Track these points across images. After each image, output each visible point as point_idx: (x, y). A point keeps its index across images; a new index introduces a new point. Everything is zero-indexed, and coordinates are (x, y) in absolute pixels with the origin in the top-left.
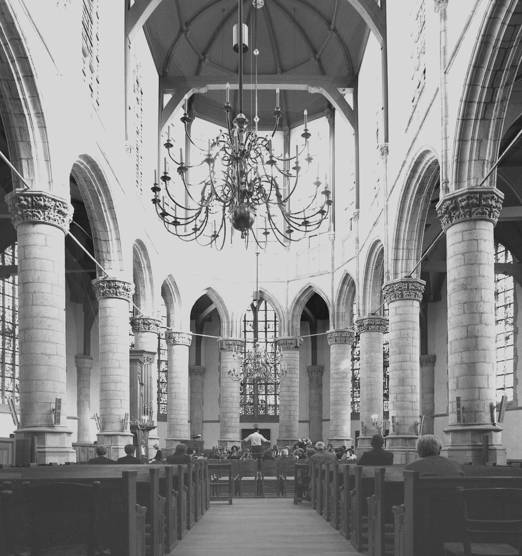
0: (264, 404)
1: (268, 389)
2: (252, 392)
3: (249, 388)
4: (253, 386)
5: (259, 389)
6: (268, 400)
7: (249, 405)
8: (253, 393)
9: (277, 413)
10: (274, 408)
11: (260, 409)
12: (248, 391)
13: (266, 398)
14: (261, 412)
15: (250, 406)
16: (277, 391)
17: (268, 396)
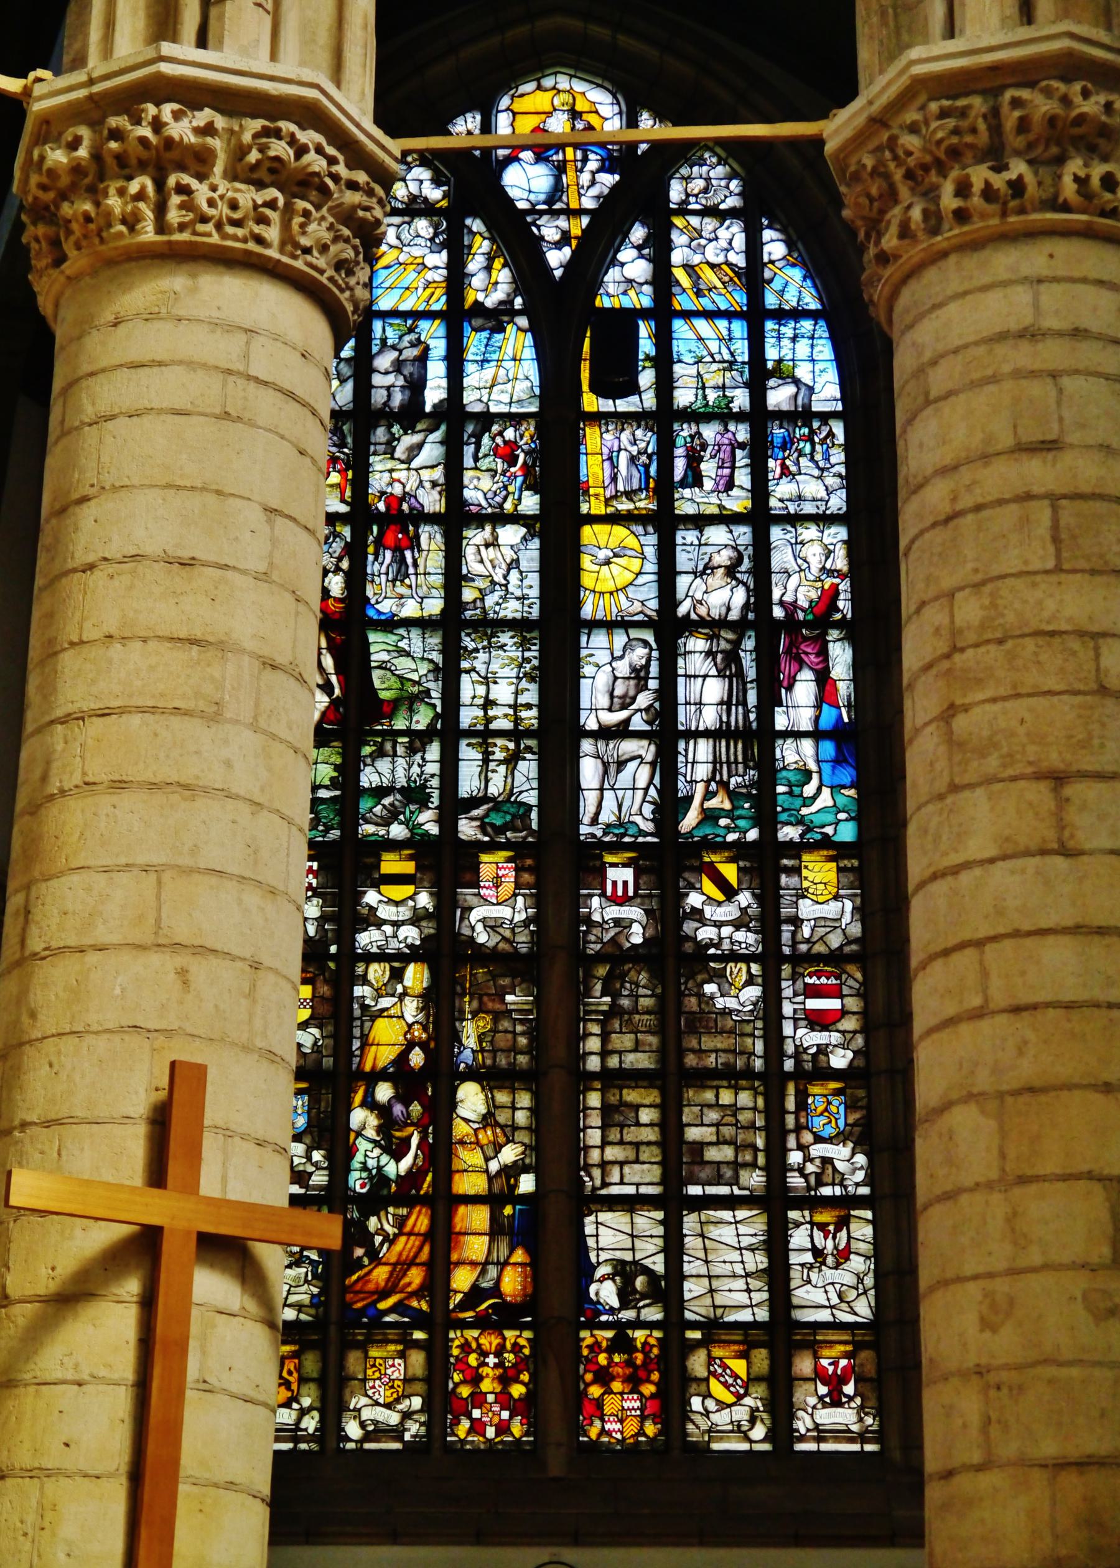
0: (654, 1314)
1: (693, 1134)
2: (512, 1172)
3: (488, 1120)
4: (524, 1099)
5: (594, 1137)
6: (690, 1267)
7: (482, 1323)
8: (527, 1184)
9: (803, 1423)
10: (761, 1358)
11: (604, 1377)
12: (470, 1157)
13: (674, 1247)
14: (611, 1405)
15: (489, 1341)
16: (795, 1157)
17: (690, 1222)
